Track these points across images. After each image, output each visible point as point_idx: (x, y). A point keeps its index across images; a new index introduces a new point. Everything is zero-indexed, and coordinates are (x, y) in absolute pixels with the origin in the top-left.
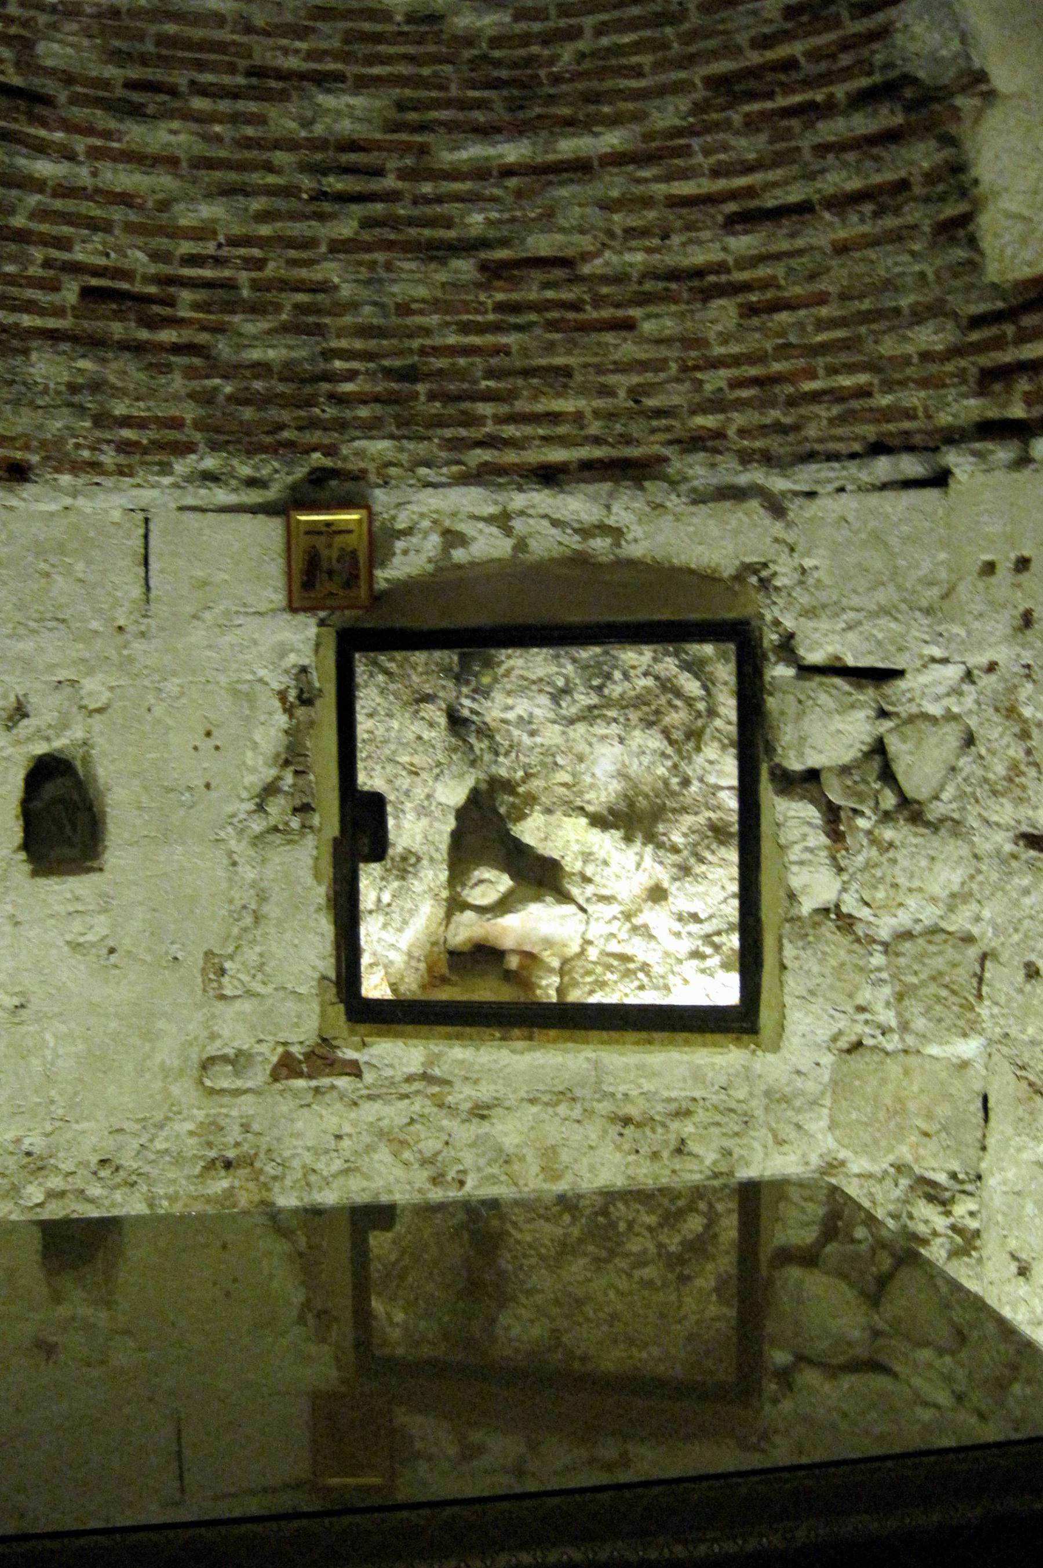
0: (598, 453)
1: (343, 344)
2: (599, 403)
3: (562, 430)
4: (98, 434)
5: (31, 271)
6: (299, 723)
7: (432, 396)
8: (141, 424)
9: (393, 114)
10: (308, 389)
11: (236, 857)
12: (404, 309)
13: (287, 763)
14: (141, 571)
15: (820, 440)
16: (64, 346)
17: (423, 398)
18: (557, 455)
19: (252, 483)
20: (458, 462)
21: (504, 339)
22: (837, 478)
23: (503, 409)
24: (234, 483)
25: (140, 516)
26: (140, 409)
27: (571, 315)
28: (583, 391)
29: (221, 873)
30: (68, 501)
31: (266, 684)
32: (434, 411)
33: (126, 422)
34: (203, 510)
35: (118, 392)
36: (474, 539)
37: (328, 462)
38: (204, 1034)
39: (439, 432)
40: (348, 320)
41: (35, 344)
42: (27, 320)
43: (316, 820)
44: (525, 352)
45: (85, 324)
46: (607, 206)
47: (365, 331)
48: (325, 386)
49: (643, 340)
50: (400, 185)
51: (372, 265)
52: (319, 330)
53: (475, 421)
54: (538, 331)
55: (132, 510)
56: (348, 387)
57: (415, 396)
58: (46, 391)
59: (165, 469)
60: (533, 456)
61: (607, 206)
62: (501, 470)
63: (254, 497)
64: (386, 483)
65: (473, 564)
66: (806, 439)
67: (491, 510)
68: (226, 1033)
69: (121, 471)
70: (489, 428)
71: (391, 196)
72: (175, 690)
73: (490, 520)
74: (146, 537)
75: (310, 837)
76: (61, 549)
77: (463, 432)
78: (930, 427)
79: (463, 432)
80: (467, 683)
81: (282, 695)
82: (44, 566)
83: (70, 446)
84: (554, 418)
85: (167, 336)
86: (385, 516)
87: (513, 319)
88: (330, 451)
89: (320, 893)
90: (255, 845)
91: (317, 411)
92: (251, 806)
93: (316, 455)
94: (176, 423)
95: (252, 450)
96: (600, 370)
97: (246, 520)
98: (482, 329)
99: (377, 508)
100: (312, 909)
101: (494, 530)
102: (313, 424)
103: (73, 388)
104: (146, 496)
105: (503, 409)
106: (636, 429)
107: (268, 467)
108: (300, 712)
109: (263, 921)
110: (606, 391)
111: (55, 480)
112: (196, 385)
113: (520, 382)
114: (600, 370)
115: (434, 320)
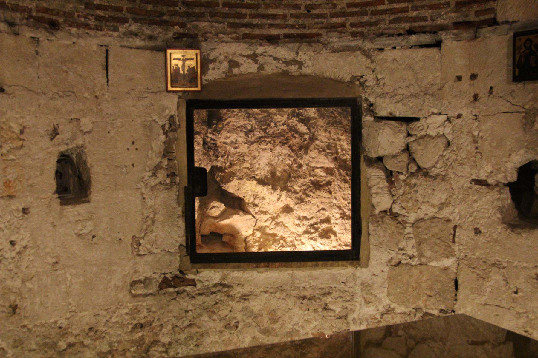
0: (292, 31)
2: (293, 11)
3: (277, 22)
6: (170, 139)
11: (144, 196)
13: (164, 156)
14: (105, 72)
15: (386, 29)
17: (221, 6)
18: (275, 32)
20: (235, 33)
22: (393, 44)
23: (254, 12)
24: (143, 37)
25: (104, 49)
30: (75, 40)
31: (157, 122)
32: (225, 11)
34: (131, 48)
36: (242, 64)
37: (181, 30)
38: (132, 271)
39: (228, 20)
43: (178, 180)
53: (242, 16)
55: (101, 46)
59: (115, 29)
63: (151, 44)
64: (206, 40)
66: (380, 28)
68: (141, 270)
69: (98, 28)
70: (247, 20)
73: (248, 57)
74: (107, 58)
75: (175, 186)
77: (237, 21)
78: (434, 24)
79: (237, 21)
81: (163, 127)
82: (65, 68)
83: (76, 16)
84: (275, 17)
86: (205, 54)
89: (179, 210)
90: (152, 190)
91: (178, 8)
92: (150, 174)
93: (177, 27)
95: (151, 23)
97: (148, 54)
99: (203, 50)
100: (176, 216)
101: (250, 61)
102: (176, 13)
104: (107, 40)
105: (254, 12)
106: (308, 22)
107: (157, 31)
108: (170, 134)
109: (156, 222)
111: (70, 30)
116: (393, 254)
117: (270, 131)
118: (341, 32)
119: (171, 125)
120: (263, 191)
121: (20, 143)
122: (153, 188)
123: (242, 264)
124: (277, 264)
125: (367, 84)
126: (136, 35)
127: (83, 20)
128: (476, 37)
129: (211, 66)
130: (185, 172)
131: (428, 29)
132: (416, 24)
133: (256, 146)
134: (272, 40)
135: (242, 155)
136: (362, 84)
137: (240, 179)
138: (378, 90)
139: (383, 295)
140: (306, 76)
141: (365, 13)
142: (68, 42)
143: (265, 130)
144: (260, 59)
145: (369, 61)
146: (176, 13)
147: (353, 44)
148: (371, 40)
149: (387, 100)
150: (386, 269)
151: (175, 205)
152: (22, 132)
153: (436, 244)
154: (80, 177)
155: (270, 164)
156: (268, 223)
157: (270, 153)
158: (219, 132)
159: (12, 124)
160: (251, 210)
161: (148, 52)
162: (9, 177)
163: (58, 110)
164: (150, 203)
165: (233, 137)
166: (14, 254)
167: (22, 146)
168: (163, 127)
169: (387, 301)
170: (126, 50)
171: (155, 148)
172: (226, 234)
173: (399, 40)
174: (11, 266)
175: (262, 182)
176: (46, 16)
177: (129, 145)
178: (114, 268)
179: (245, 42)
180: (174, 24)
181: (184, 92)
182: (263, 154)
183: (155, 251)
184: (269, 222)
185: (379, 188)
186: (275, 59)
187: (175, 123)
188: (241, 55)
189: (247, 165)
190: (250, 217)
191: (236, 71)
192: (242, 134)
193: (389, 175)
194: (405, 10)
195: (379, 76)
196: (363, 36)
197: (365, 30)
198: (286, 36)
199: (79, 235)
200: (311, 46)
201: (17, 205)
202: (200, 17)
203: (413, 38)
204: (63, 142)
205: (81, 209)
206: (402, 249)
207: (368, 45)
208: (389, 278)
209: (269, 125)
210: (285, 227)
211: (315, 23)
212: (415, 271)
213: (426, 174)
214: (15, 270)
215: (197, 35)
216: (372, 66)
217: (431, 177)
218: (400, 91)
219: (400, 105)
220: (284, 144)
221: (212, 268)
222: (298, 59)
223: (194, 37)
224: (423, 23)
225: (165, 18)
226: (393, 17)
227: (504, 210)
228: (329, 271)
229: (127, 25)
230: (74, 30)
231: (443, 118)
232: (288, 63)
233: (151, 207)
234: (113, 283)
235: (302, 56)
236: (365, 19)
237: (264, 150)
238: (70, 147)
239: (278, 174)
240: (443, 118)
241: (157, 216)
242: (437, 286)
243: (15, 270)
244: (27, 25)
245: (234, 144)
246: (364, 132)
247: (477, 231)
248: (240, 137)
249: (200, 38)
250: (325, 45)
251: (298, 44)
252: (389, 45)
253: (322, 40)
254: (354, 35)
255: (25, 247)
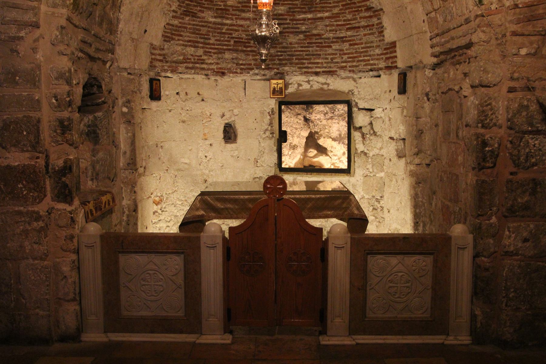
1: (280, 50)
2: (325, 61)
3: (319, 65)
4: (237, 67)
5: (225, 39)
7: (296, 59)
8: (244, 65)
9: (288, 10)
10: (274, 58)
12: (291, 44)
13: (269, 125)
16: (231, 52)
18: (318, 70)
19: (264, 75)
21: (309, 49)
23: (309, 61)
25: (244, 81)
26: (244, 62)
27: (320, 45)
28: (323, 58)
29: (257, 144)
30: (232, 79)
33: (242, 64)
35: (240, 59)
37: (277, 71)
40: (281, 46)
41: (226, 51)
42: (225, 47)
43: (275, 135)
44: (312, 51)
45: (235, 48)
46: (327, 26)
47: (283, 47)
48: (277, 57)
49: (333, 50)
50: (290, 22)
51: (285, 36)
52: (276, 47)
53: (304, 64)
54: (315, 48)
56: (281, 58)
57: (293, 59)
58: (228, 59)
59: (249, 73)
60: (313, 70)
61: (327, 26)
62: (308, 73)
63: (264, 78)
65: (303, 90)
67: (307, 80)
69: (241, 73)
70: (306, 65)
71: (289, 24)
72: (250, 112)
73: (306, 82)
76: (230, 87)
77: (301, 66)
79: (301, 66)
80: (308, 111)
81: (269, 113)
82: (227, 90)
84: (318, 63)
85: (249, 49)
87: (310, 45)
88: (278, 69)
89: (275, 148)
91: (275, 62)
92: (263, 132)
93: (275, 70)
94: (250, 64)
96: (326, 55)
98: (305, 47)
99: (286, 79)
102: (275, 64)
103: (233, 59)
104: (245, 78)
105: (309, 61)
106: (332, 65)
108: (272, 116)
110: (327, 59)
112: (254, 58)
113: (312, 57)
114: (326, 55)
115: (296, 46)
116: (365, 171)
117: (336, 113)
118: (345, 70)
119: (272, 112)
120: (335, 144)
121: (210, 119)
122: (264, 139)
123: (300, 173)
124: (315, 173)
125: (355, 93)
126: (257, 74)
127: (235, 70)
128: (391, 74)
129: (290, 86)
130: (277, 132)
131: (376, 69)
132: (372, 67)
133: (330, 121)
134: (317, 74)
135: (324, 126)
136: (353, 93)
137: (324, 138)
138: (359, 96)
139: (360, 190)
140: (330, 90)
141: (354, 61)
142: (229, 80)
143: (333, 113)
144: (311, 82)
145: (355, 83)
146: (275, 64)
147: (349, 75)
148: (356, 74)
149: (362, 101)
150: (362, 178)
151: (273, 146)
152: (210, 115)
153: (378, 166)
154: (235, 133)
155: (339, 130)
156: (337, 161)
157: (338, 125)
158: (311, 114)
159: (207, 112)
160: (329, 154)
161: (263, 81)
162: (205, 132)
163: (224, 107)
164: (262, 145)
165: (318, 116)
166: (206, 161)
167: (210, 121)
168: (269, 113)
169: (362, 193)
170: (253, 81)
171: (265, 122)
172: (317, 166)
173: (367, 73)
174: (205, 165)
175: (334, 140)
176: (220, 70)
177: (254, 120)
178: (246, 171)
179: (305, 75)
180: (274, 69)
181: (278, 98)
182: (334, 125)
183: (264, 165)
184: (337, 161)
185: (359, 141)
186: (318, 82)
187: (274, 111)
188: (303, 81)
189: (327, 131)
190: (328, 157)
191: (301, 88)
192: (322, 115)
193: (363, 136)
194: (369, 60)
195: (360, 90)
196: (353, 71)
197: (354, 69)
198: (323, 72)
199: (232, 156)
200: (333, 76)
201: (208, 142)
202: (285, 65)
203: (371, 73)
204: (226, 119)
205: (233, 145)
206: (367, 169)
207: (355, 76)
208: (363, 182)
209: (335, 110)
210: (343, 163)
211: (335, 66)
212: (372, 179)
213: (375, 135)
214: (207, 167)
215: (284, 73)
216: (356, 85)
217: (377, 136)
218: (367, 97)
219: (366, 103)
220: (343, 120)
221: (288, 174)
222: (327, 82)
223: (283, 74)
224: (375, 67)
225: (270, 66)
226: (364, 63)
227: (399, 150)
228: (339, 178)
229: (253, 71)
230: (231, 75)
231: (381, 109)
232: (323, 84)
233: (263, 147)
234: (246, 177)
235: (329, 81)
236: (354, 64)
237: (335, 123)
238: (229, 121)
239: (342, 136)
240: (381, 109)
241: (265, 151)
242: (379, 185)
243: (207, 167)
244: (212, 75)
245: (319, 119)
246: (354, 115)
247: (390, 160)
248: (322, 116)
249: (285, 74)
250: (338, 76)
251: (327, 76)
252: (363, 76)
253: (338, 73)
254: (350, 71)
255: (211, 159)
